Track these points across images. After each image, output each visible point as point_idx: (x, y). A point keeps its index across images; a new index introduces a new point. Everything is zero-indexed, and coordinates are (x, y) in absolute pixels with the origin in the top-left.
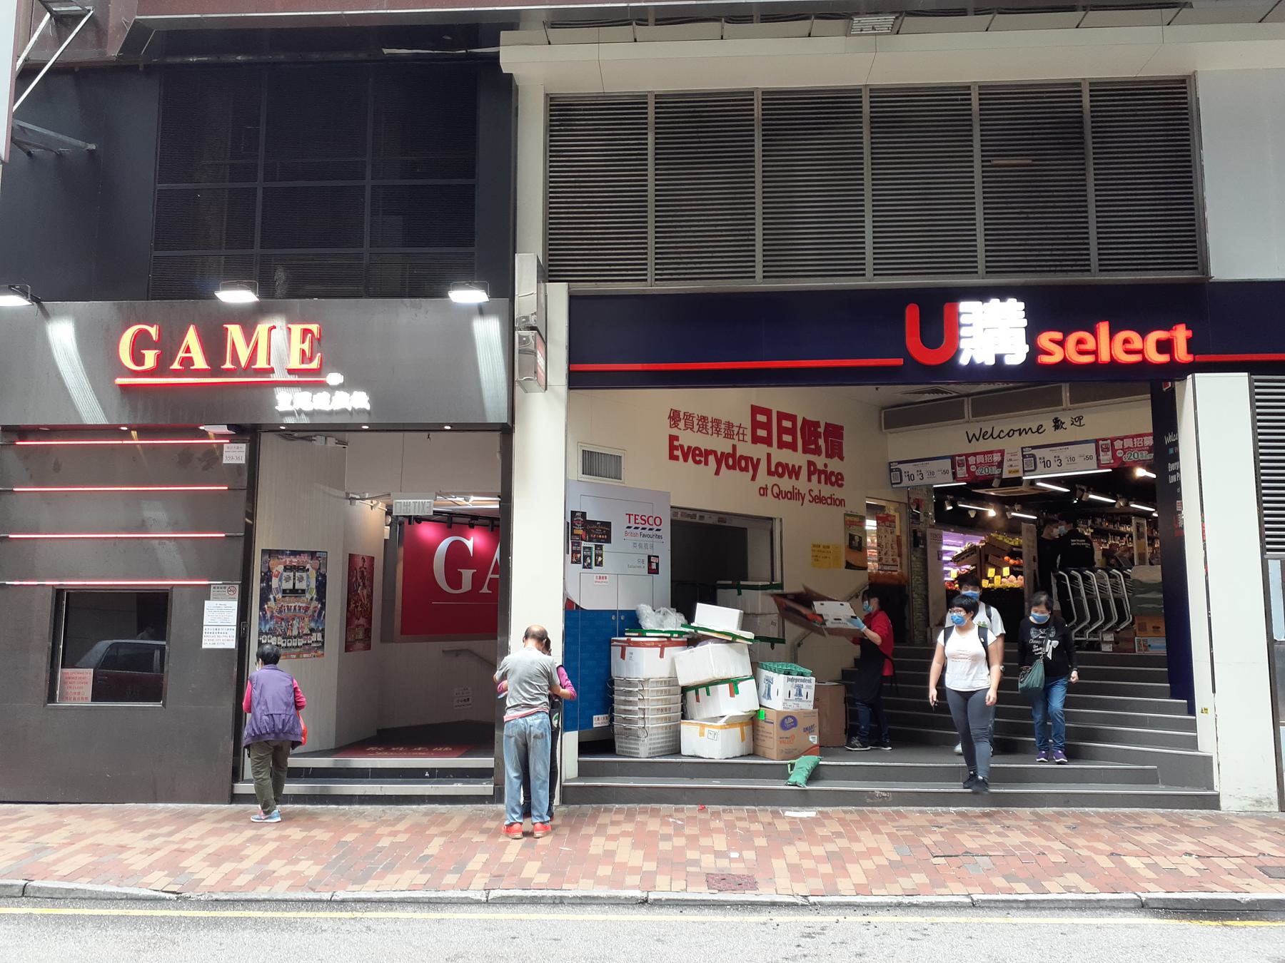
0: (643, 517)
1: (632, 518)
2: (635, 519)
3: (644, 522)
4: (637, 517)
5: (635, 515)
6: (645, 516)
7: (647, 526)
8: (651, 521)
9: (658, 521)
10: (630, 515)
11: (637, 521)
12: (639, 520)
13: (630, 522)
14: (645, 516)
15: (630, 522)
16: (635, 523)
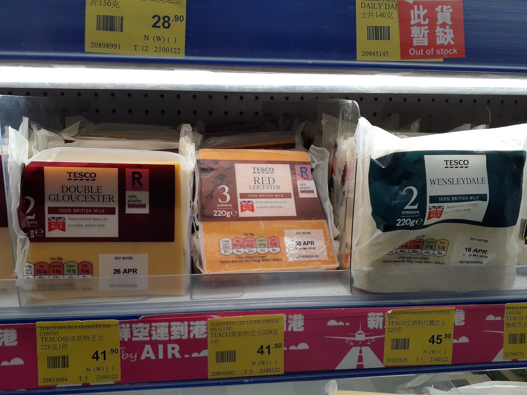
0: (456, 161)
1: (449, 162)
2: (451, 163)
3: (456, 164)
4: (452, 161)
5: (450, 161)
6: (457, 161)
7: (459, 165)
8: (462, 162)
9: (466, 162)
10: (447, 161)
11: (452, 164)
12: (453, 163)
13: (447, 165)
14: (457, 161)
15: (447, 165)
16: (451, 165)
